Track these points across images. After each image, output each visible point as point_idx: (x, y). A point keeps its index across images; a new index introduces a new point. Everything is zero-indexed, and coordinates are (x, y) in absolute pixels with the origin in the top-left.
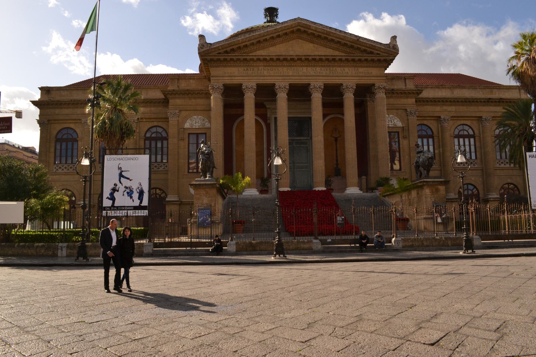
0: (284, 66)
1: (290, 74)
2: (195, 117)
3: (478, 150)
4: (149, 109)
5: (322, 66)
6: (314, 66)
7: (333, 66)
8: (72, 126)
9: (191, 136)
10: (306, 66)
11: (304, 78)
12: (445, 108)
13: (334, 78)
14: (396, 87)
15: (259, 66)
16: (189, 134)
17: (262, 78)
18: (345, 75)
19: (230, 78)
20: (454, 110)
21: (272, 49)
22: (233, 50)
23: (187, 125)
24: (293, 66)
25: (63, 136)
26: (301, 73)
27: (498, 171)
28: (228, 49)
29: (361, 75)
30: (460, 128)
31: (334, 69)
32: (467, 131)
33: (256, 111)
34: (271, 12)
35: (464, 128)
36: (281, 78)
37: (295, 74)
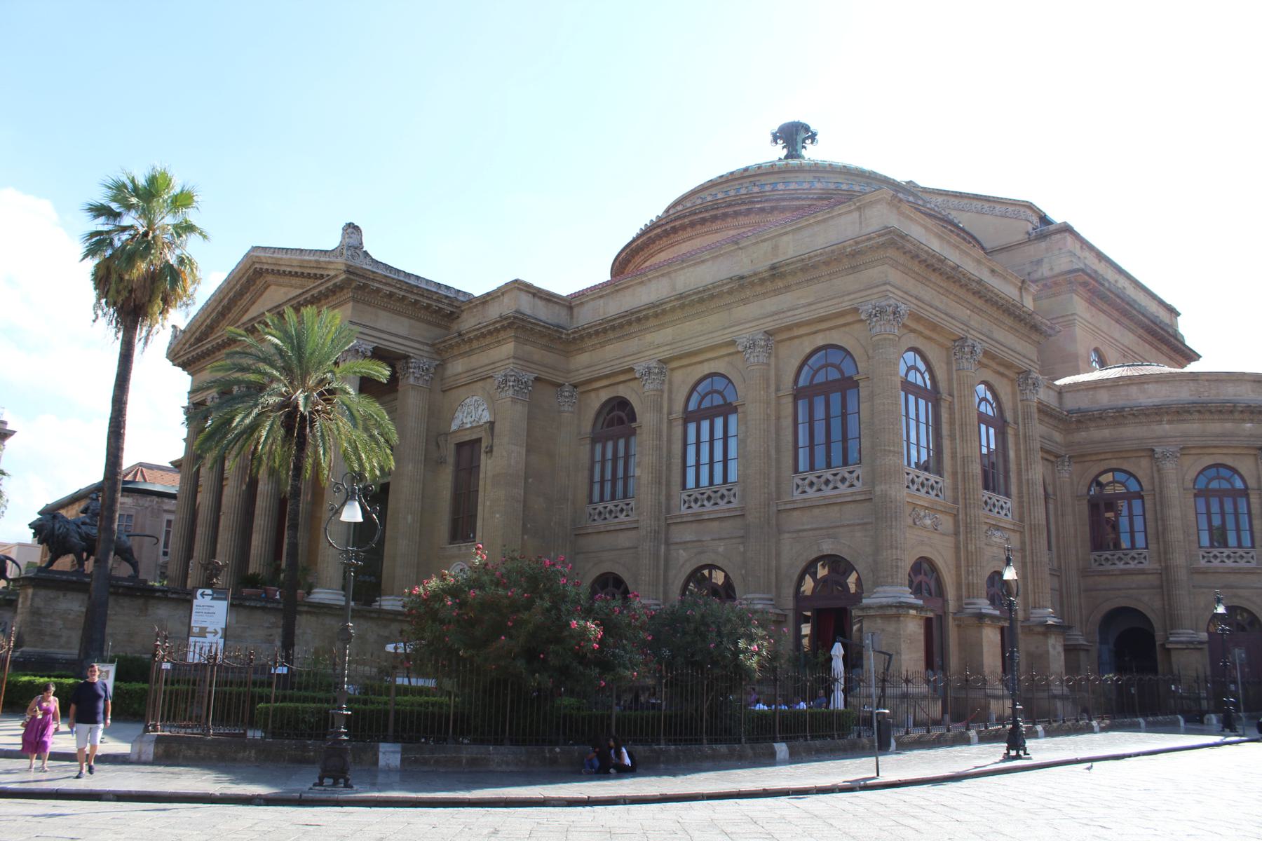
27: (795, 514)
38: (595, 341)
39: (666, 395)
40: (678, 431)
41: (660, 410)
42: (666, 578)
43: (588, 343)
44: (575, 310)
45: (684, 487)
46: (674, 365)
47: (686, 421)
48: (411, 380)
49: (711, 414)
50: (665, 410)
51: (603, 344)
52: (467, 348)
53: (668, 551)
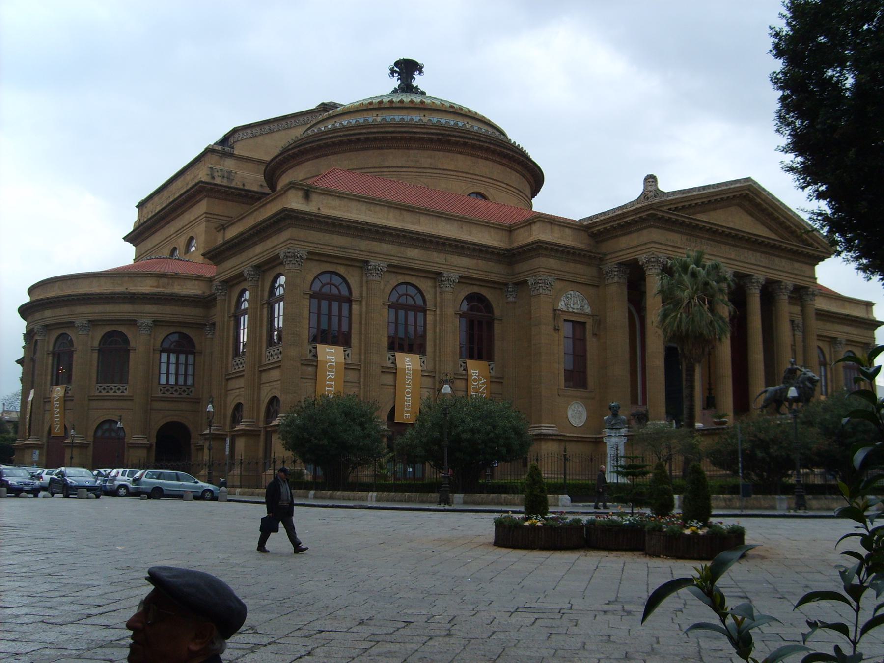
1: (732, 257)
2: (572, 292)
3: (829, 383)
4: (475, 261)
5: (762, 252)
8: (341, 270)
11: (746, 265)
15: (702, 238)
21: (712, 213)
23: (561, 305)
25: (322, 287)
26: (742, 259)
28: (680, 205)
29: (795, 272)
33: (629, 294)
34: (407, 69)
37: (737, 258)
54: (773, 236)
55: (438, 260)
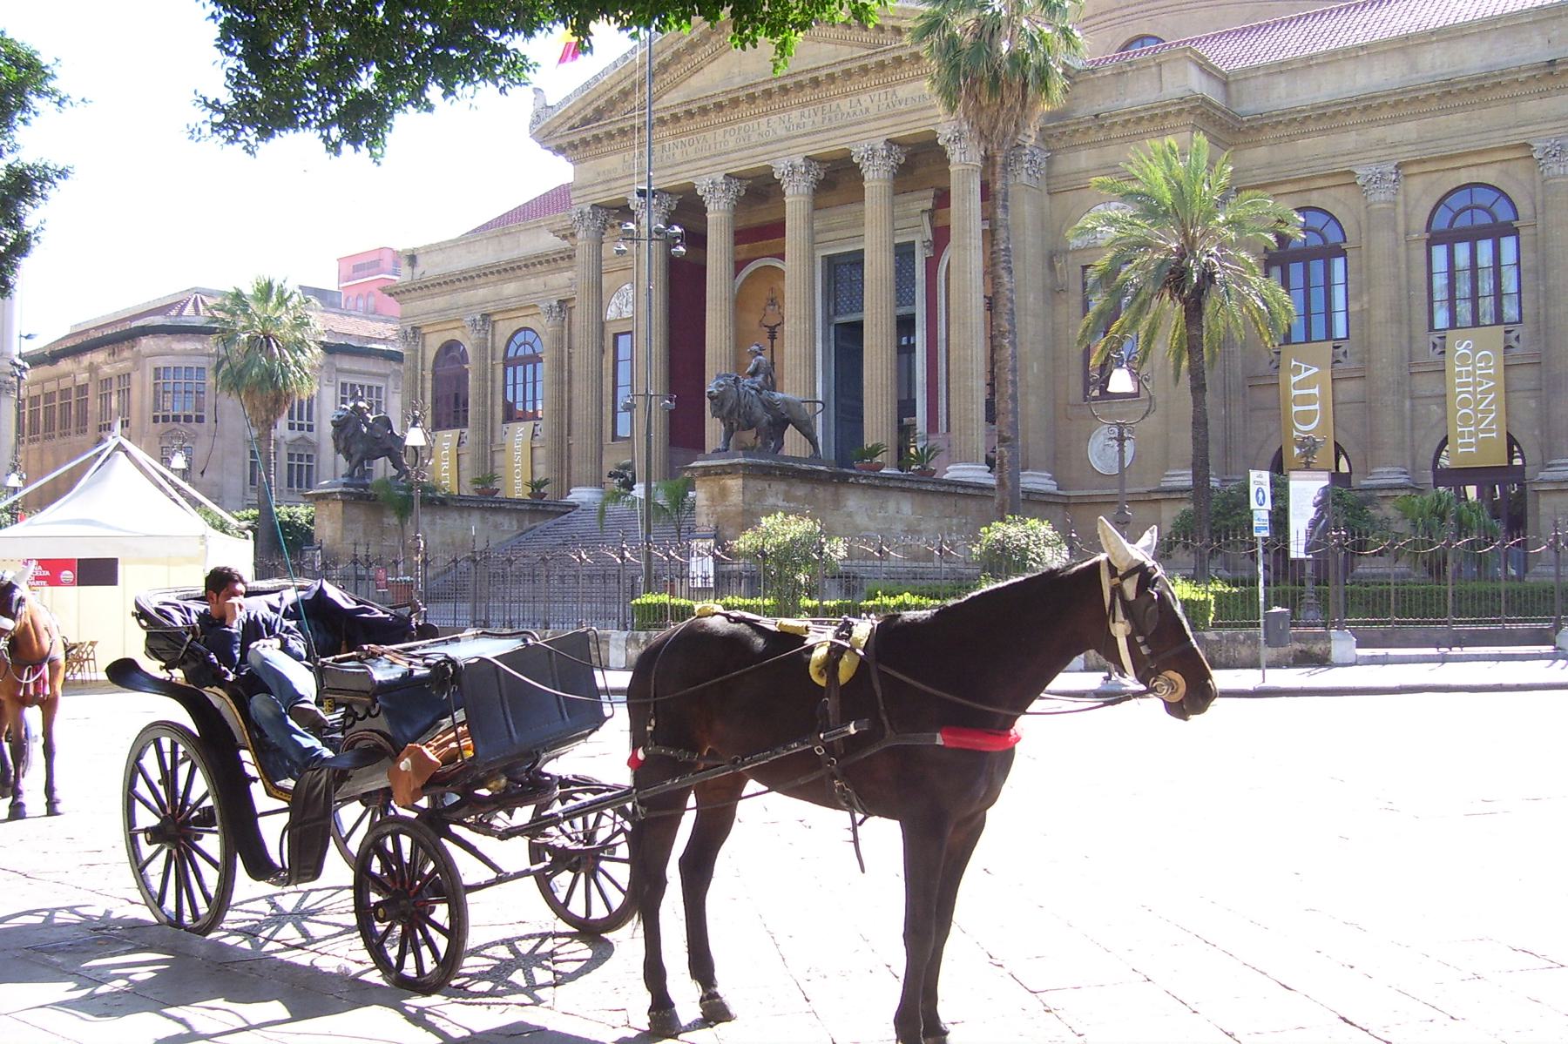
0: (716, 126)
5: (804, 105)
6: (784, 109)
7: (830, 99)
9: (621, 338)
10: (766, 114)
12: (1376, 133)
13: (831, 134)
14: (1127, 103)
16: (616, 336)
17: (670, 171)
18: (861, 117)
19: (605, 187)
20: (1414, 136)
22: (599, 114)
24: (736, 121)
28: (589, 111)
30: (1457, 202)
31: (834, 104)
32: (1488, 210)
35: (1478, 201)
36: (707, 163)
38: (1282, 131)
39: (1400, 209)
40: (1420, 255)
41: (1395, 230)
42: (1412, 440)
43: (1270, 135)
44: (1233, 88)
45: (1431, 328)
46: (1414, 169)
47: (1431, 243)
48: (1024, 178)
49: (1472, 236)
50: (1401, 229)
51: (1291, 138)
52: (1101, 136)
53: (1413, 405)
54: (845, 52)
55: (534, 289)
